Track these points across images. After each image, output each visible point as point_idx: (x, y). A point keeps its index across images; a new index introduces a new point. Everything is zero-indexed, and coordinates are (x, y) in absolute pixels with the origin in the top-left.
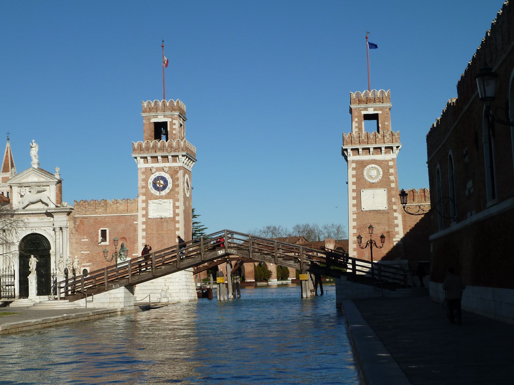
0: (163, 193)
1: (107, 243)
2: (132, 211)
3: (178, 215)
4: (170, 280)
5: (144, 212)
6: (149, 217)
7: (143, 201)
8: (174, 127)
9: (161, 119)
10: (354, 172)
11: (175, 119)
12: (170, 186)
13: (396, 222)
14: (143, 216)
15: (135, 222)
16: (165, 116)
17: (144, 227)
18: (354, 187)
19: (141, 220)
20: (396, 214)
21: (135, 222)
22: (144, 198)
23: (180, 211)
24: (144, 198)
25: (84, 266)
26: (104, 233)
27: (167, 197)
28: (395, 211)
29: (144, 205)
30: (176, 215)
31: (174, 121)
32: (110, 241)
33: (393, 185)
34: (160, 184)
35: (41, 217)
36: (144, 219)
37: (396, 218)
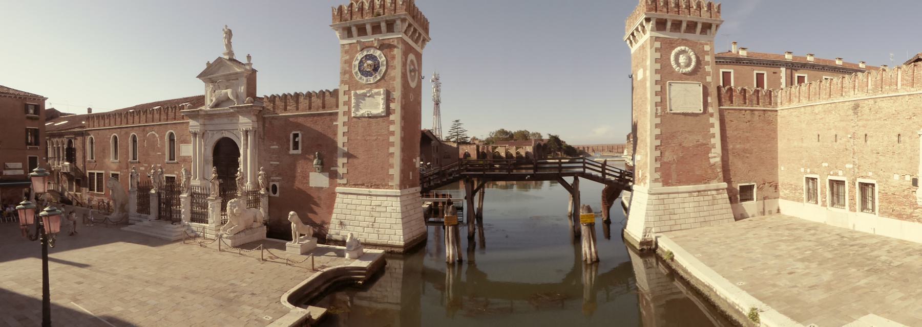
0: (372, 80)
1: (299, 151)
2: (331, 108)
4: (378, 209)
5: (346, 108)
7: (345, 93)
10: (658, 55)
13: (712, 130)
14: (345, 114)
18: (658, 77)
19: (341, 119)
20: (712, 120)
23: (396, 106)
25: (273, 181)
27: (377, 84)
28: (712, 115)
29: (346, 98)
30: (388, 111)
33: (709, 79)
37: (712, 125)
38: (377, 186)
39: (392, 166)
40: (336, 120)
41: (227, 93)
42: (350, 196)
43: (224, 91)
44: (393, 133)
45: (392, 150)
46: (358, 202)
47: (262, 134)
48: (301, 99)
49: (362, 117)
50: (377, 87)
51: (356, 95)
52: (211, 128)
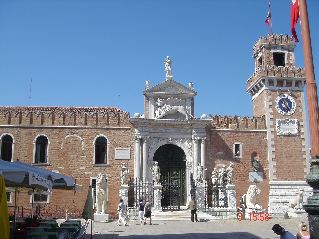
0: (289, 113)
3: (303, 133)
5: (272, 130)
6: (278, 134)
7: (271, 119)
8: (291, 57)
9: (279, 51)
11: (291, 51)
12: (294, 106)
14: (272, 133)
15: (265, 139)
16: (283, 48)
17: (273, 143)
21: (265, 139)
22: (272, 116)
24: (272, 116)
26: (237, 147)
29: (272, 123)
31: (291, 53)
32: (243, 155)
34: (286, 104)
35: (178, 129)
36: (273, 136)
38: (297, 180)
39: (305, 166)
40: (266, 137)
41: (178, 109)
42: (279, 187)
43: (174, 107)
44: (304, 146)
45: (304, 156)
46: (286, 190)
47: (209, 143)
48: (240, 121)
49: (284, 136)
50: (292, 118)
51: (280, 122)
52: (157, 135)
